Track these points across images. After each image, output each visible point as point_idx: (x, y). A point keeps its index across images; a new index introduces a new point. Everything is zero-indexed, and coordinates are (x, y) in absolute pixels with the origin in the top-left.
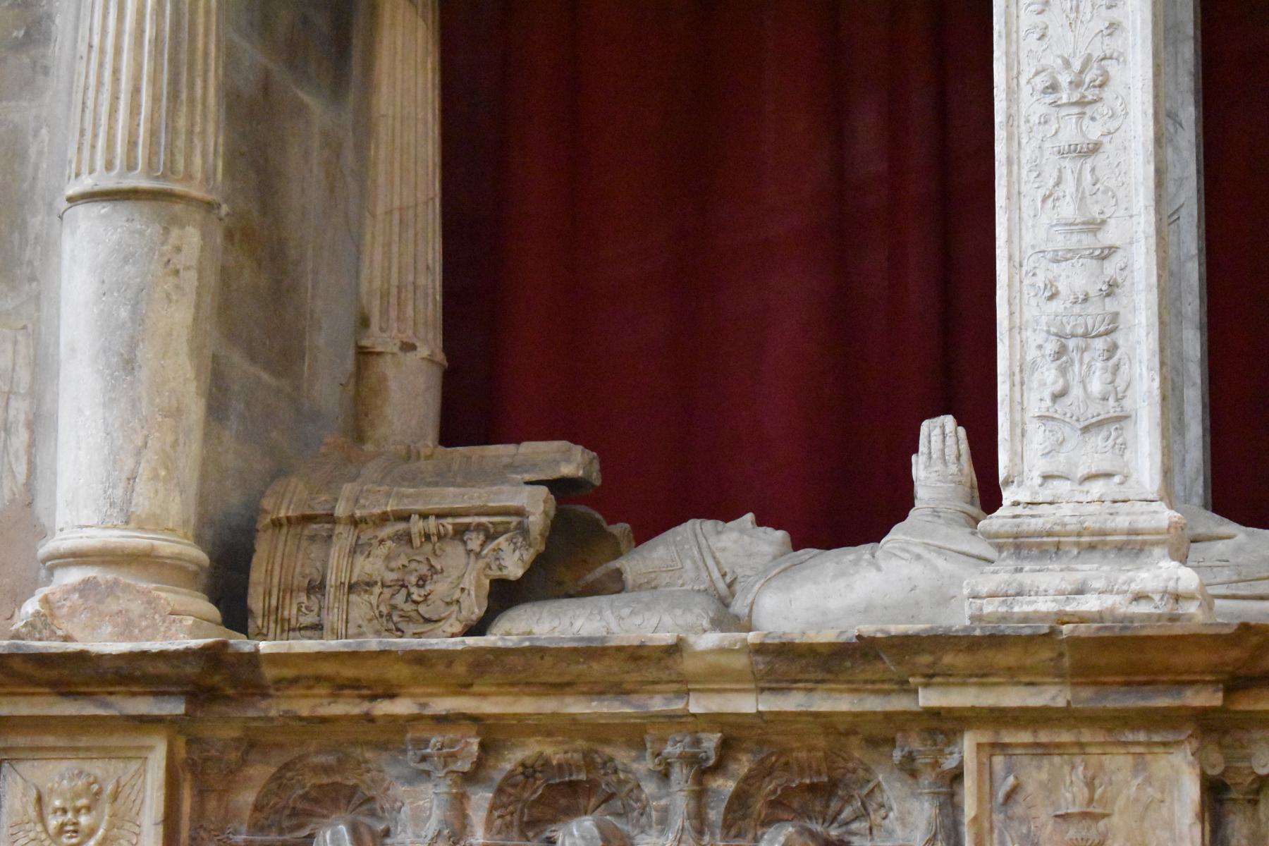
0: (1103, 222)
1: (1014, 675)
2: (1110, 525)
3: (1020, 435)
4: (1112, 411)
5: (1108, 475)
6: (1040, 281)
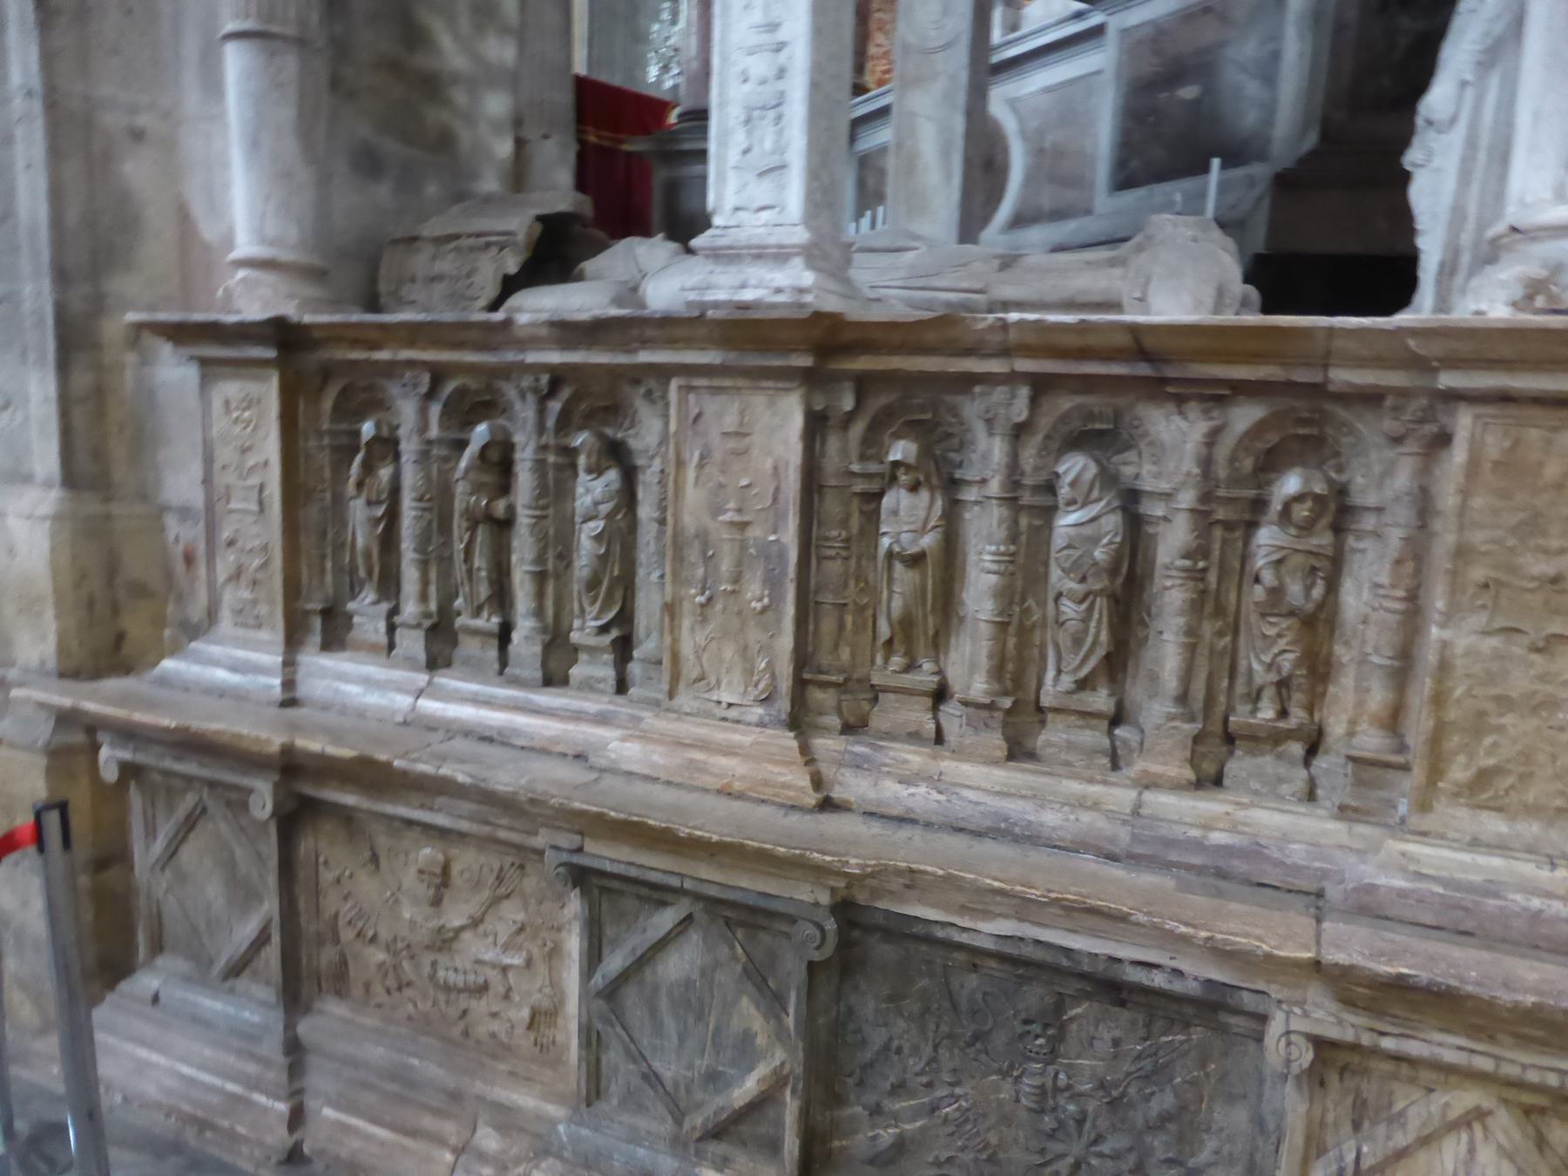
6: (740, 67)
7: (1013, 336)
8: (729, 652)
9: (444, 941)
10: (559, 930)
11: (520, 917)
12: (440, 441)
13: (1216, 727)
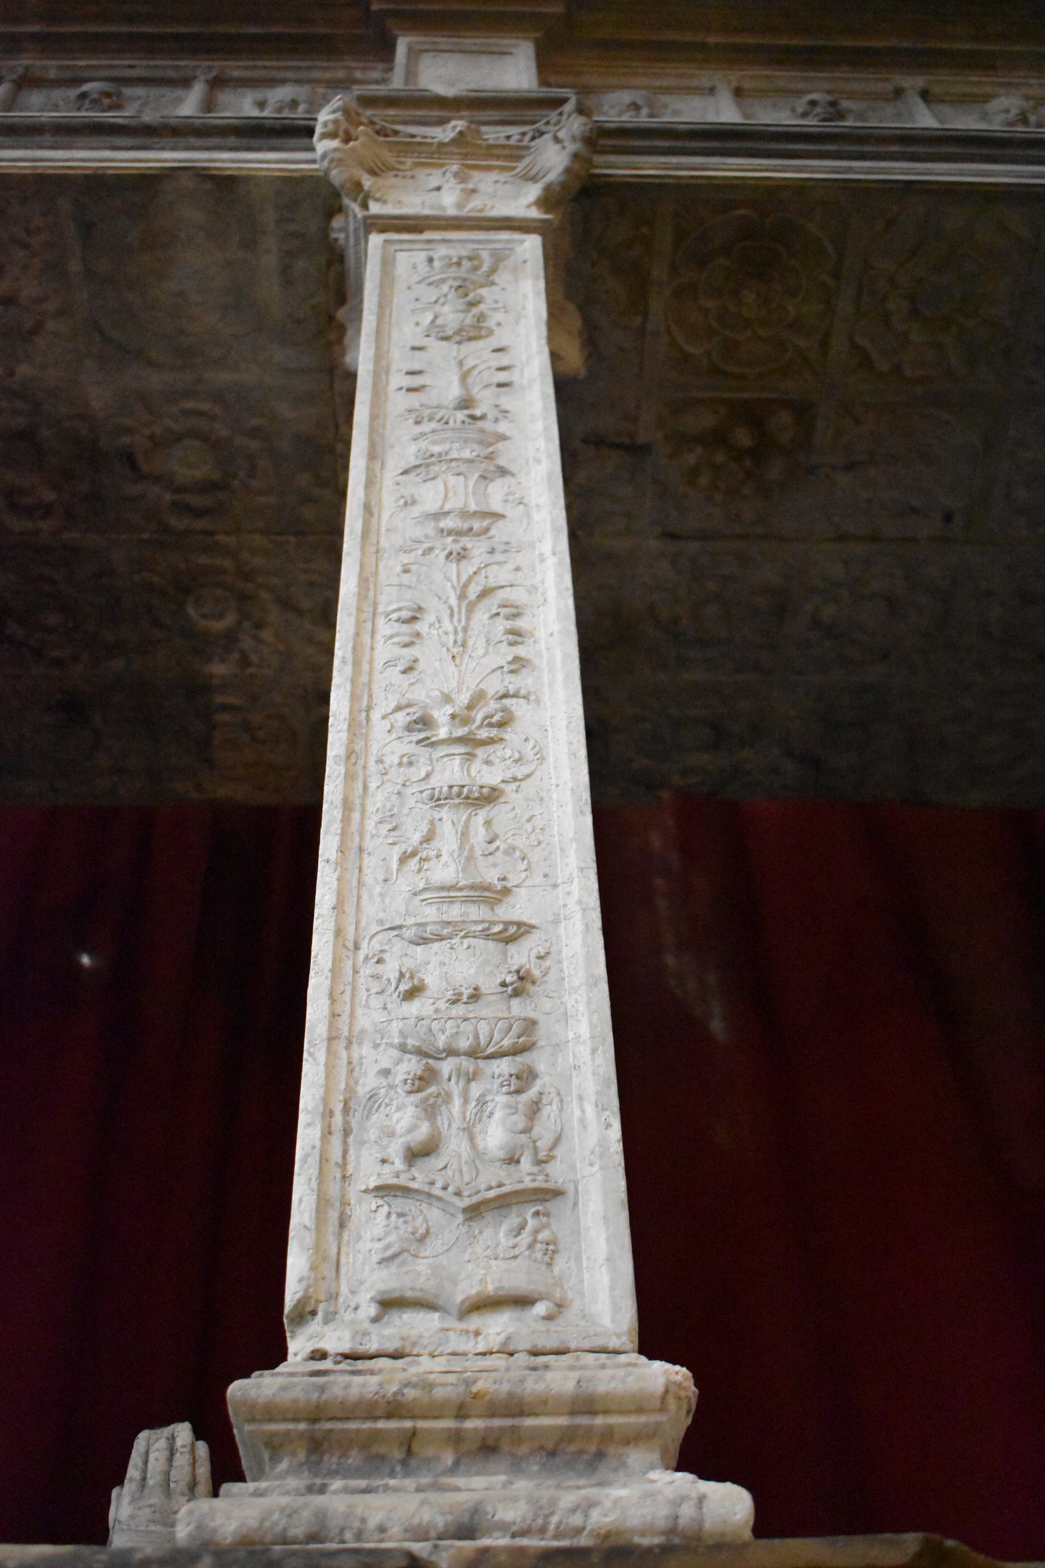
0: (506, 891)
2: (533, 1386)
3: (337, 1223)
4: (528, 1179)
5: (522, 1301)
6: (391, 969)
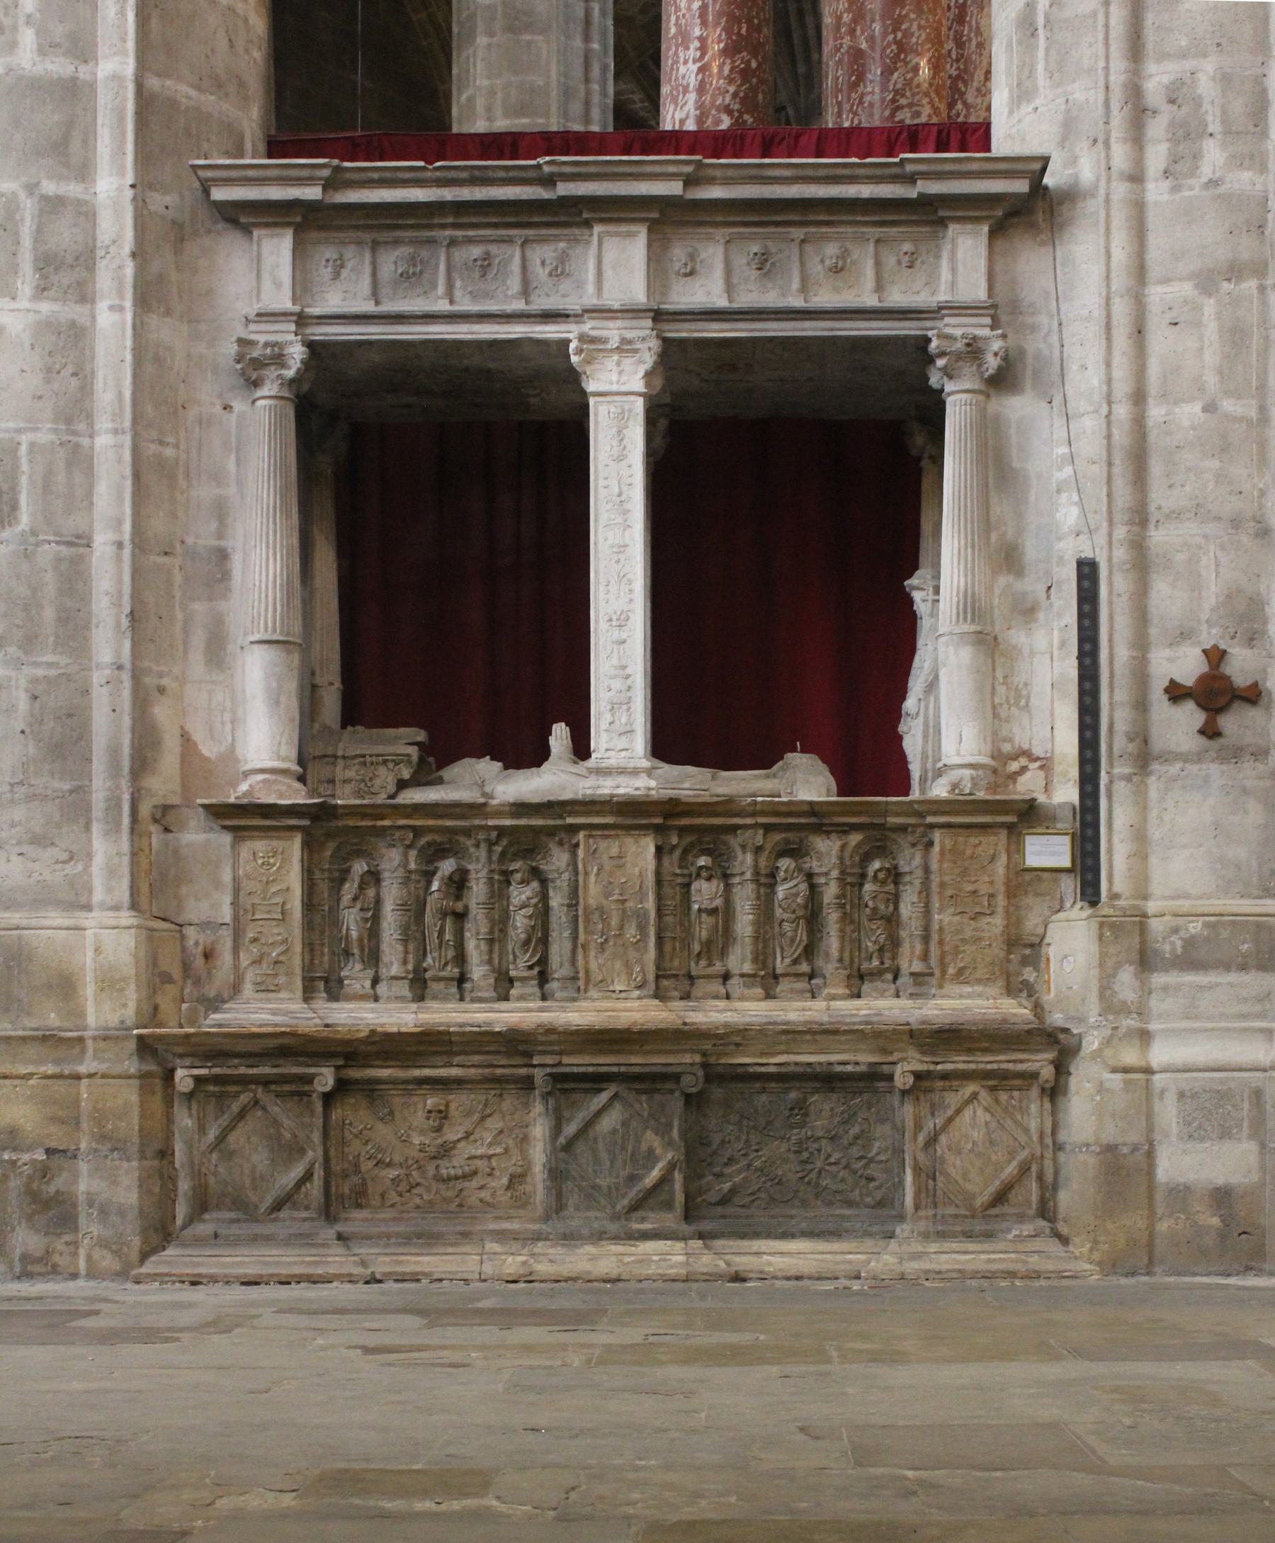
1: (598, 813)
7: (758, 807)
8: (618, 965)
9: (445, 1151)
10: (527, 1126)
11: (500, 1125)
12: (416, 871)
13: (855, 973)
